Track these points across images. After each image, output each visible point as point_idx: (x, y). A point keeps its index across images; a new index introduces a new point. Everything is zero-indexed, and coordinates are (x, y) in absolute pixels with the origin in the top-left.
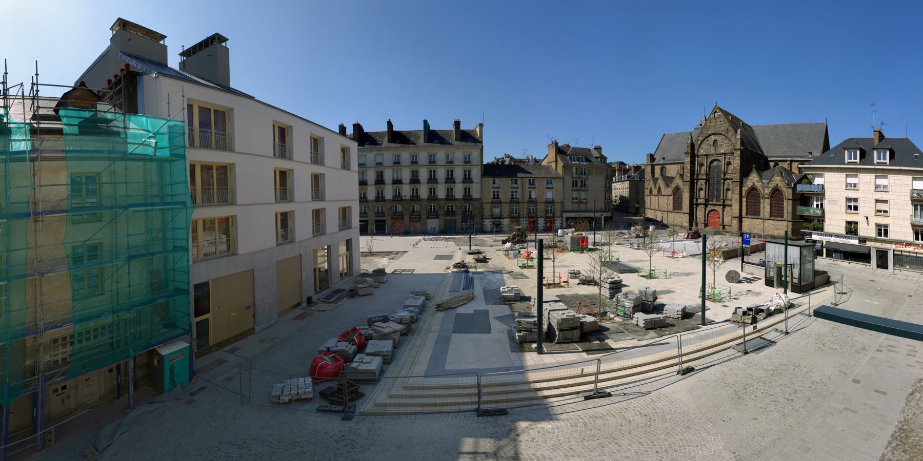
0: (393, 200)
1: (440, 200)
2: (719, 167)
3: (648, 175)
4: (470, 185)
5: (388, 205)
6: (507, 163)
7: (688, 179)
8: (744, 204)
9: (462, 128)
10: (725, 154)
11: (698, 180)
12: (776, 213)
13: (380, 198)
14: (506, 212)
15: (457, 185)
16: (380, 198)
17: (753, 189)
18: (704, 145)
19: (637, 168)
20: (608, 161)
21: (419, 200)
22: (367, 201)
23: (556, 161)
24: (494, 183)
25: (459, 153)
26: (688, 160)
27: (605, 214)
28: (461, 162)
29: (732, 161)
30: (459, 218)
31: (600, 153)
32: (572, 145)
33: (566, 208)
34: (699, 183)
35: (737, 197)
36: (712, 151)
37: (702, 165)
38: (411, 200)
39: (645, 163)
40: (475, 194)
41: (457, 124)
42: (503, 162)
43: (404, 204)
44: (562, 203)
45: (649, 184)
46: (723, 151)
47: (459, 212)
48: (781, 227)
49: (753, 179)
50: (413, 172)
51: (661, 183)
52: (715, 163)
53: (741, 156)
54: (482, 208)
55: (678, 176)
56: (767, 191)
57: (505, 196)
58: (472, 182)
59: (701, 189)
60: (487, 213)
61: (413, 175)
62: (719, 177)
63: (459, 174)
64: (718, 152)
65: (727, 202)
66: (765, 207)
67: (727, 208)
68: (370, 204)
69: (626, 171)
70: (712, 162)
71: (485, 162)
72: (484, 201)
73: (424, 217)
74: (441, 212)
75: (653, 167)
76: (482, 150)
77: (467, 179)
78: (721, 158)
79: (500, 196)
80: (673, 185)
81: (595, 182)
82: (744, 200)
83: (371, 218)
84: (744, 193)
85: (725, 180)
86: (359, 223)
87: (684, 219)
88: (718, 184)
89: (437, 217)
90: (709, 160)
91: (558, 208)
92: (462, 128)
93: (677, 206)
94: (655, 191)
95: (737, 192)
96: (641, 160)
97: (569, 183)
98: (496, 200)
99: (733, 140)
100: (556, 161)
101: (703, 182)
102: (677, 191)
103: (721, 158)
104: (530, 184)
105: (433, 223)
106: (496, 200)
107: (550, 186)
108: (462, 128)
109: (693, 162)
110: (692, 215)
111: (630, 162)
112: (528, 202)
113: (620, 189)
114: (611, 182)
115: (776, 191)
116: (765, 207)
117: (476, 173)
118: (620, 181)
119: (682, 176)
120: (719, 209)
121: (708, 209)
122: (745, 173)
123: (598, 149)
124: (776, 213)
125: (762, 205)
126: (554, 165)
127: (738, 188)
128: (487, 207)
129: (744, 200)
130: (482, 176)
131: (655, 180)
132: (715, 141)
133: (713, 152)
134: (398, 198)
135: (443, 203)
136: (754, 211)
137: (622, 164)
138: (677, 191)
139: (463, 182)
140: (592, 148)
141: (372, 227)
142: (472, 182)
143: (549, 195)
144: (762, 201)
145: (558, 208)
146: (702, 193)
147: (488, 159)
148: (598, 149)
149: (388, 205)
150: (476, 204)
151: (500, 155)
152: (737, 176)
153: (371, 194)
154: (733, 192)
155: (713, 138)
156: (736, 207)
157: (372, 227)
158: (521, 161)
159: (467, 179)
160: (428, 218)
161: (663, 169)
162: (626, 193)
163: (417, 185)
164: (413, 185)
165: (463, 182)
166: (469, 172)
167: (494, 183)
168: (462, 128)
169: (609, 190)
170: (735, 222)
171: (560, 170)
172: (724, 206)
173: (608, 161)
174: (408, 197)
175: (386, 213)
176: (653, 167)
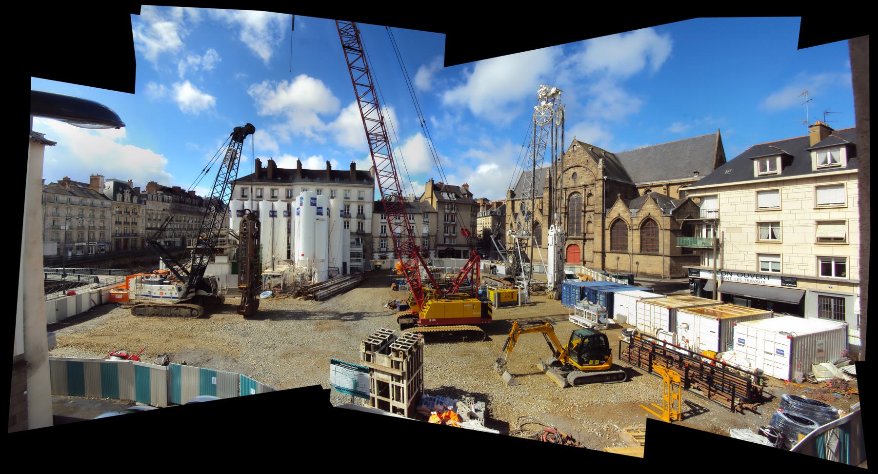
2: (579, 199)
3: (509, 211)
6: (393, 200)
9: (357, 169)
12: (648, 247)
17: (618, 220)
19: (499, 204)
20: (474, 197)
25: (354, 191)
26: (546, 194)
28: (356, 199)
29: (593, 192)
31: (467, 191)
35: (600, 229)
36: (571, 183)
41: (353, 165)
42: (390, 199)
44: (436, 236)
45: (509, 219)
46: (583, 183)
48: (657, 265)
49: (619, 209)
51: (521, 218)
52: (574, 196)
56: (637, 222)
62: (579, 210)
63: (354, 210)
64: (578, 184)
65: (587, 236)
66: (634, 239)
69: (489, 207)
70: (571, 195)
71: (376, 200)
77: (361, 214)
78: (581, 190)
81: (464, 216)
82: (608, 233)
84: (607, 225)
85: (585, 212)
88: (579, 217)
90: (568, 193)
91: (432, 240)
92: (358, 168)
94: (515, 226)
95: (600, 224)
96: (503, 197)
97: (442, 218)
103: (581, 190)
108: (358, 168)
111: (493, 199)
113: (484, 223)
114: (476, 217)
115: (648, 223)
116: (634, 239)
117: (368, 209)
119: (541, 210)
121: (568, 243)
122: (609, 203)
123: (466, 186)
124: (648, 247)
125: (629, 238)
127: (600, 220)
129: (608, 233)
131: (516, 215)
136: (619, 246)
137: (485, 200)
144: (629, 233)
152: (599, 208)
154: (595, 225)
155: (572, 171)
159: (361, 214)
162: (489, 226)
165: (357, 217)
168: (357, 169)
169: (474, 226)
170: (598, 257)
171: (435, 205)
172: (585, 240)
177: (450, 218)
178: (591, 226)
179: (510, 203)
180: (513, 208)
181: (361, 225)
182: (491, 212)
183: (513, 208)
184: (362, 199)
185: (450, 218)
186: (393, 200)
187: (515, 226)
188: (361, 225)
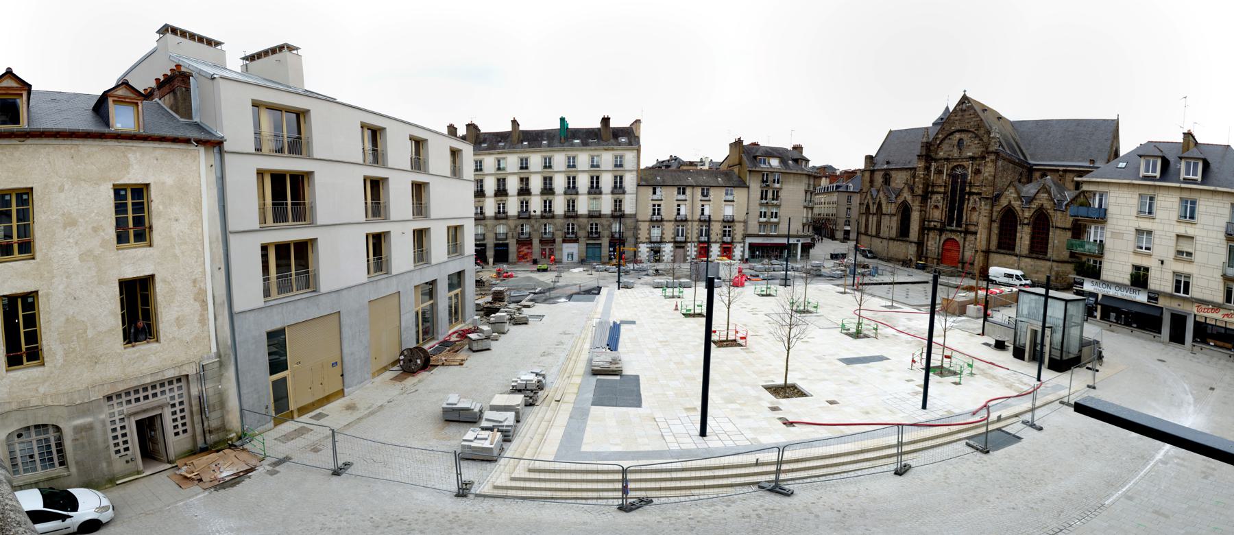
0: (519, 217)
1: (582, 216)
2: (964, 176)
4: (621, 197)
5: (512, 223)
7: (920, 192)
8: (995, 231)
10: (972, 158)
11: (933, 193)
13: (501, 215)
14: (669, 236)
15: (603, 196)
16: (501, 215)
18: (945, 146)
19: (850, 175)
20: (811, 164)
21: (553, 217)
22: (484, 218)
23: (740, 164)
24: (654, 193)
26: (922, 164)
27: (802, 241)
28: (611, 167)
30: (605, 242)
32: (762, 144)
33: (750, 231)
34: (934, 197)
37: (940, 172)
38: (542, 217)
39: (862, 167)
40: (628, 208)
43: (533, 221)
47: (606, 233)
50: (545, 179)
52: (959, 171)
53: (995, 162)
54: (636, 229)
55: (906, 189)
57: (668, 212)
58: (624, 193)
59: (936, 207)
60: (643, 235)
61: (545, 184)
62: (963, 190)
64: (964, 155)
65: (972, 228)
67: (970, 238)
68: (488, 222)
70: (953, 169)
71: (642, 167)
72: (639, 217)
73: (559, 240)
74: (582, 234)
75: (872, 172)
76: (639, 151)
77: (618, 188)
79: (663, 212)
80: (900, 201)
81: (792, 194)
83: (490, 242)
85: (971, 194)
86: (473, 248)
87: (912, 250)
89: (576, 240)
93: (904, 232)
94: (873, 209)
98: (655, 218)
99: (985, 139)
100: (740, 164)
101: (939, 197)
102: (905, 212)
104: (703, 195)
105: (570, 250)
106: (657, 221)
107: (730, 198)
109: (928, 169)
110: (920, 244)
112: (700, 221)
117: (630, 181)
118: (826, 191)
119: (912, 190)
120: (959, 238)
123: (798, 148)
126: (736, 169)
127: (988, 207)
128: (644, 227)
129: (995, 225)
130: (639, 185)
132: (961, 139)
133: (956, 155)
134: (525, 215)
135: (585, 221)
138: (905, 212)
139: (612, 193)
140: (790, 148)
141: (490, 254)
142: (624, 193)
143: (729, 211)
145: (739, 230)
146: (937, 214)
147: (648, 161)
148: (798, 148)
149: (512, 223)
150: (629, 222)
151: (665, 157)
153: (490, 208)
156: (982, 235)
157: (490, 254)
158: (691, 164)
159: (618, 188)
160: (564, 241)
161: (887, 179)
163: (550, 197)
164: (545, 197)
165: (612, 193)
166: (621, 178)
167: (654, 193)
172: (967, 232)
173: (811, 164)
174: (538, 213)
175: (510, 235)
176: (872, 172)
177: (770, 195)
178: (975, 217)
179: (867, 175)
180: (872, 182)
181: (618, 203)
182: (838, 187)
183: (872, 182)
184: (598, 166)
185: (770, 195)
186: (674, 168)
187: (873, 209)
188: (618, 203)
